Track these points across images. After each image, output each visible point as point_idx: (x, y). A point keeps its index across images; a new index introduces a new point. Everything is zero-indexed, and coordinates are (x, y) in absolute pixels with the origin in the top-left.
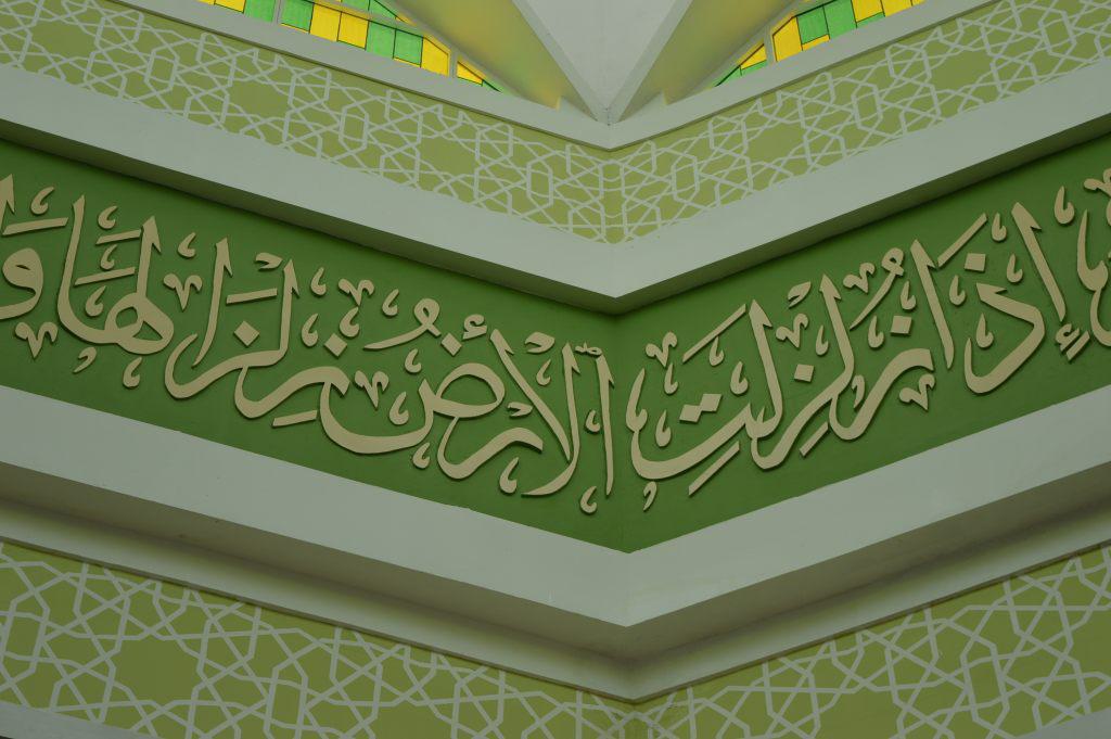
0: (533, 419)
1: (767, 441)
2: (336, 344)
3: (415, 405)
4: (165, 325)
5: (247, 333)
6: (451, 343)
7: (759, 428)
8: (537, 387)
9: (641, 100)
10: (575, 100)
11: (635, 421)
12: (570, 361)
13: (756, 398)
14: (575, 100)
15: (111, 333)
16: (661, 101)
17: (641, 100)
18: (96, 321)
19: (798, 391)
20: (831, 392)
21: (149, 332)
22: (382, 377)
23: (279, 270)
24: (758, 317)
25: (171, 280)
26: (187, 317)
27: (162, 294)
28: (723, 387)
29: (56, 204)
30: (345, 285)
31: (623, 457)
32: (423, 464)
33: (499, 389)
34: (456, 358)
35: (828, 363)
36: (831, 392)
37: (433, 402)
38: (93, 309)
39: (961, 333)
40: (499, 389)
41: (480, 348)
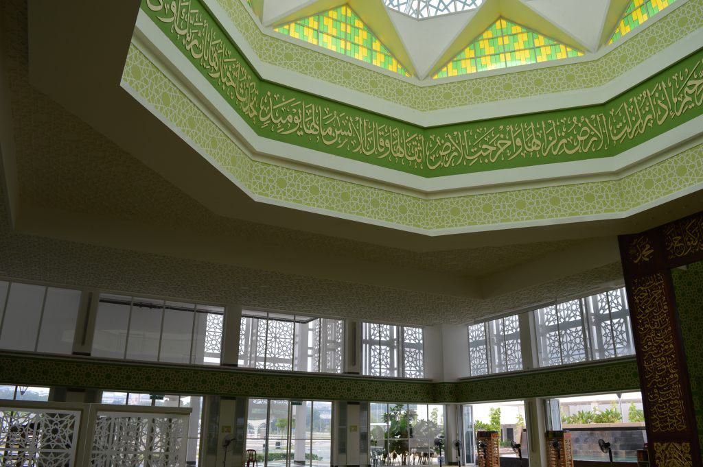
0: (595, 135)
1: (630, 133)
2: (563, 134)
3: (577, 140)
4: (539, 143)
5: (551, 138)
6: (580, 125)
7: (629, 131)
8: (594, 127)
9: (600, 46)
11: (610, 128)
12: (598, 118)
13: (627, 124)
15: (534, 148)
16: (603, 46)
18: (530, 147)
19: (634, 123)
20: (638, 124)
21: (538, 145)
22: (571, 137)
23: (552, 123)
24: (626, 107)
25: (538, 134)
26: (542, 140)
27: (537, 137)
28: (622, 121)
29: (519, 128)
30: (562, 121)
31: (610, 136)
32: (580, 151)
33: (589, 131)
34: (582, 127)
35: (637, 118)
36: (638, 124)
37: (580, 138)
38: (530, 145)
39: (656, 112)
40: (589, 131)
41: (584, 124)
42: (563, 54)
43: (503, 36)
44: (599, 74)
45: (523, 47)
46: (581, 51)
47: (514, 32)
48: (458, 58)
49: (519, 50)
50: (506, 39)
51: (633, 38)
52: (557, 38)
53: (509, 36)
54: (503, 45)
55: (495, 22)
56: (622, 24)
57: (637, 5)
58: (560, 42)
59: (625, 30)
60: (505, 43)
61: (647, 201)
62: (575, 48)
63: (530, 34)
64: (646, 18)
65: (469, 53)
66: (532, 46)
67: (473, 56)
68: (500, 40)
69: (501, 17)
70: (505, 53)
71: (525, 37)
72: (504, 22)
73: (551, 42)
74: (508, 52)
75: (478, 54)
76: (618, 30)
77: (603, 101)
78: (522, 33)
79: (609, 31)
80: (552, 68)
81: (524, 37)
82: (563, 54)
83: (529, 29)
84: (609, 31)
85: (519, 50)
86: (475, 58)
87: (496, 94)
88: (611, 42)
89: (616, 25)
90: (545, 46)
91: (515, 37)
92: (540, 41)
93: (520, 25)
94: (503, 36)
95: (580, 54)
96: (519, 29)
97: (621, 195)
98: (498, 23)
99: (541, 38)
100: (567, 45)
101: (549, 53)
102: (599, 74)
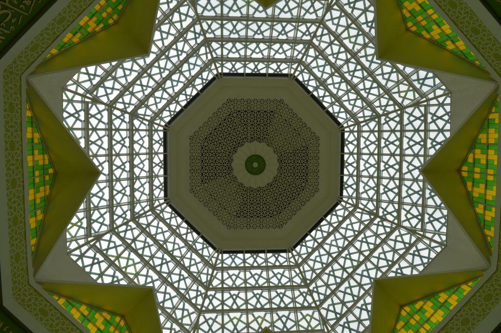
9: (489, 260)
10: (484, 270)
14: (484, 270)
17: (489, 260)
45: (433, 311)
49: (432, 315)
53: (416, 313)
56: (487, 232)
59: (490, 233)
63: (432, 299)
66: (440, 304)
71: (430, 304)
73: (452, 291)
74: (424, 324)
80: (466, 304)
85: (432, 315)
89: (485, 237)
91: (422, 310)
96: (421, 303)
98: (403, 313)
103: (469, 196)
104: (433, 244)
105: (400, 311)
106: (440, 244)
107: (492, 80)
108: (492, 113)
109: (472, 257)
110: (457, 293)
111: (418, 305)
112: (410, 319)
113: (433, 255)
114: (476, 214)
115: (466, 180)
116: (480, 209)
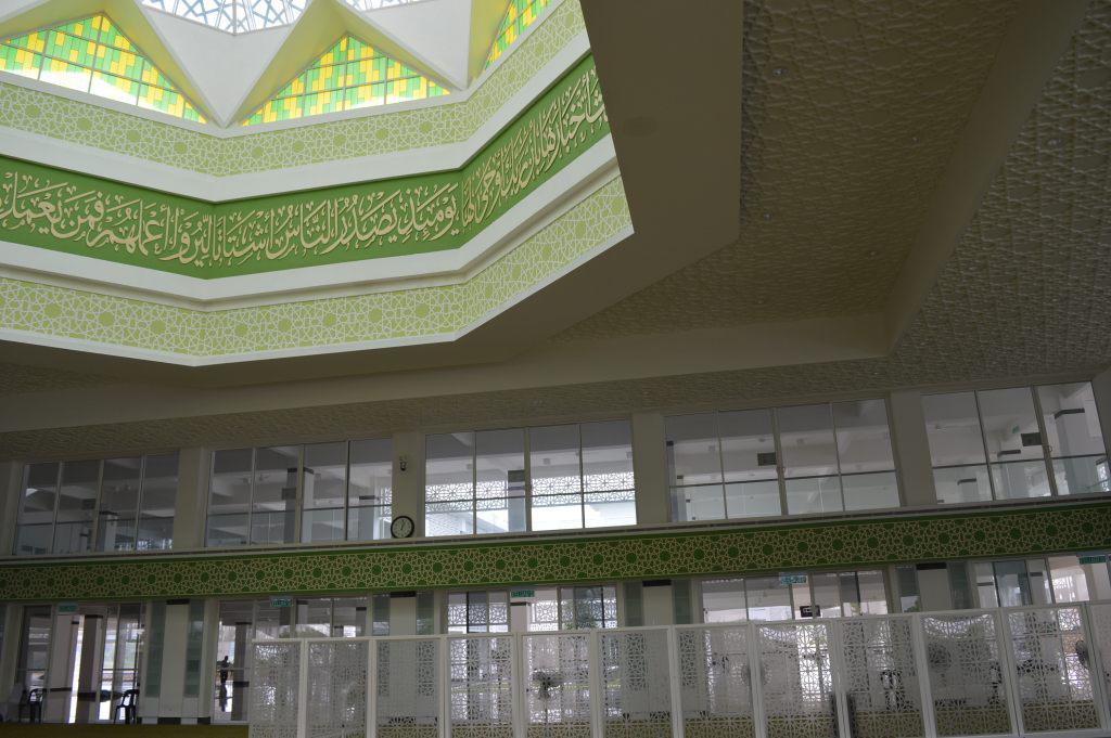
42: (176, 108)
43: (98, 43)
44: (221, 158)
46: (205, 115)
47: (117, 45)
48: (15, 42)
50: (102, 49)
51: (278, 131)
52: (176, 82)
54: (95, 57)
55: (91, 16)
56: (269, 106)
57: (294, 92)
58: (178, 89)
59: (270, 116)
60: (99, 55)
61: (233, 352)
62: (200, 108)
64: (299, 116)
65: (35, 42)
66: (138, 78)
67: (40, 49)
68: (91, 47)
69: (103, 14)
70: (93, 69)
72: (106, 22)
73: (167, 85)
75: (48, 53)
76: (260, 112)
77: (215, 199)
78: (128, 52)
79: (248, 109)
80: (159, 124)
81: (127, 62)
82: (176, 108)
83: (140, 52)
84: (248, 109)
86: (43, 55)
87: (63, 130)
88: (247, 124)
89: (261, 105)
90: (156, 87)
92: (151, 75)
93: (129, 39)
94: (98, 43)
95: (201, 120)
96: (126, 45)
97: (203, 335)
98: (96, 21)
99: (154, 72)
100: (188, 99)
101: (158, 102)
102: (221, 158)
103: (312, 64)
104: (229, 11)
105: (96, 14)
106: (234, 22)
107: (470, 81)
108: (428, 81)
109: (227, 88)
110: (168, 93)
111: (121, 41)
112: (93, 42)
113: (212, 20)
114: (289, 83)
115: (336, 49)
116: (297, 87)
